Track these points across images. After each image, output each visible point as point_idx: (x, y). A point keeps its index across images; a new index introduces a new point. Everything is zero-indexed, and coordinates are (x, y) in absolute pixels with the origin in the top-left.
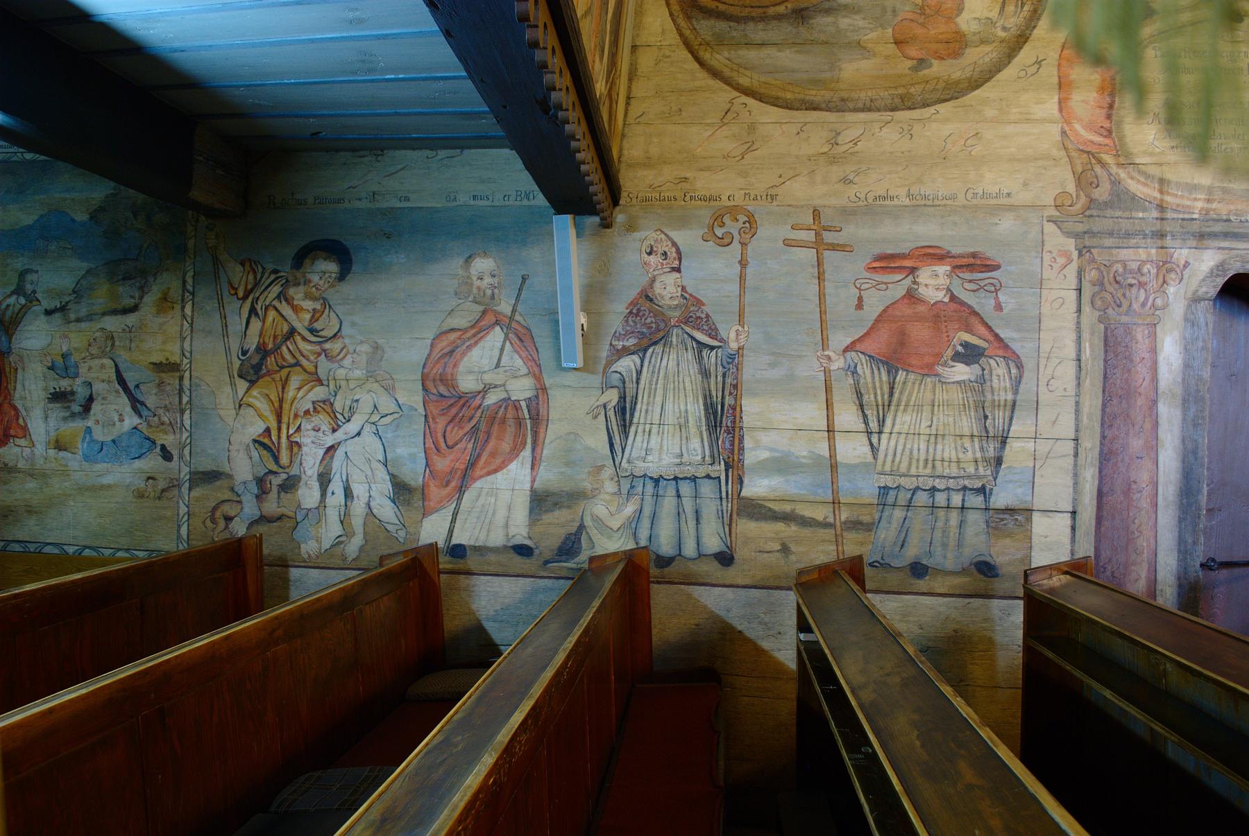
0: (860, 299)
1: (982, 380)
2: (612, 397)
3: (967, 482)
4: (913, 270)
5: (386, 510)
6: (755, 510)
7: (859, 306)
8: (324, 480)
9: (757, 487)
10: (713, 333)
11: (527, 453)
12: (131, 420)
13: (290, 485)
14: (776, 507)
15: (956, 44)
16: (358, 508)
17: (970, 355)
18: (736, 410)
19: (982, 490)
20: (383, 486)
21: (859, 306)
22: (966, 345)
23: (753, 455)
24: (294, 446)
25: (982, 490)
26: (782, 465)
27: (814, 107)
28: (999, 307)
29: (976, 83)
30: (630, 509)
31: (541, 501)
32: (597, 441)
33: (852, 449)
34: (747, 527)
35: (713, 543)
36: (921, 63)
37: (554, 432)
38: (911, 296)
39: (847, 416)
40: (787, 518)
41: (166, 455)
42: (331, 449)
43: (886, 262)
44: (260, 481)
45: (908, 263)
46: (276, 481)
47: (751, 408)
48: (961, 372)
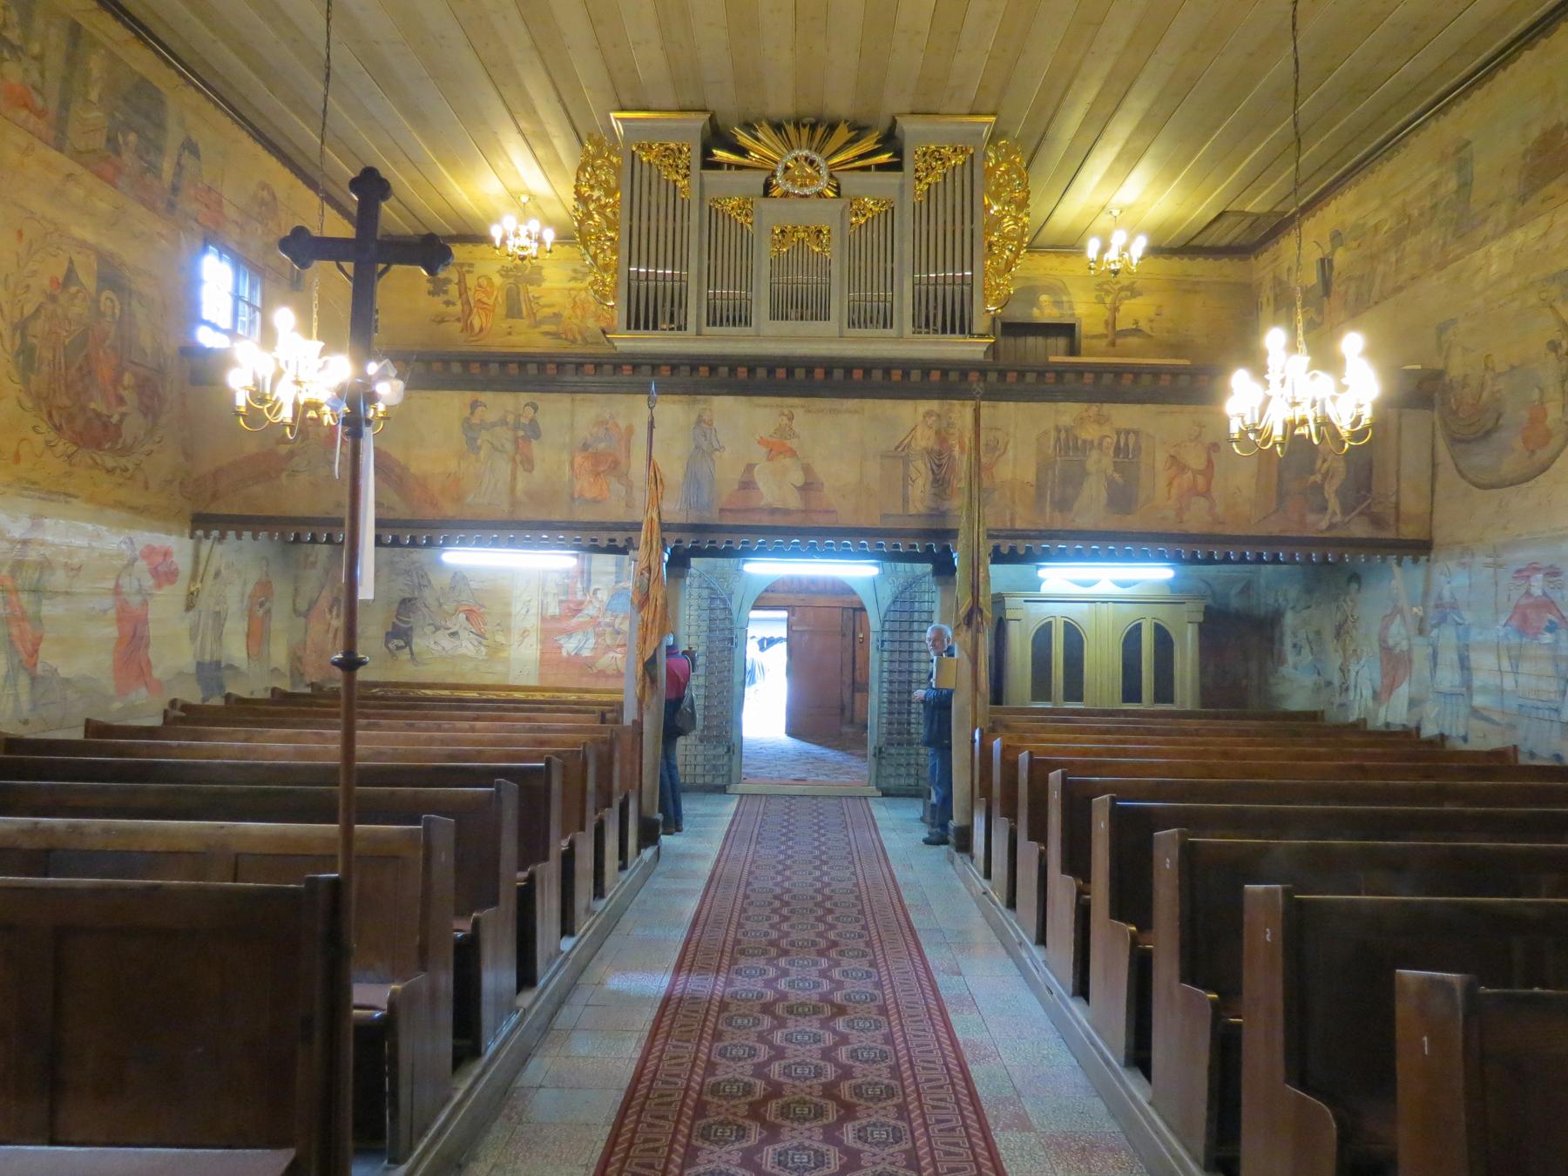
0: (1509, 596)
1: (1557, 642)
2: (1430, 650)
3: (1551, 705)
4: (1529, 577)
5: (1370, 703)
6: (1475, 712)
7: (1509, 599)
8: (1356, 686)
9: (1478, 701)
10: (1461, 618)
11: (1407, 678)
12: (1310, 658)
13: (1347, 689)
14: (1485, 713)
15: (1549, 435)
16: (1363, 703)
17: (1552, 628)
18: (1468, 657)
19: (1557, 710)
20: (1370, 692)
21: (1509, 599)
22: (1550, 621)
23: (1476, 683)
24: (1349, 670)
25: (1557, 710)
26: (1485, 690)
27: (1492, 486)
28: (1563, 598)
29: (1553, 460)
30: (1437, 709)
31: (1413, 703)
32: (1427, 672)
33: (1509, 683)
34: (1476, 724)
35: (1462, 733)
36: (1533, 452)
37: (1416, 666)
38: (1528, 594)
39: (1506, 665)
40: (1487, 719)
41: (1319, 674)
42: (1357, 673)
43: (1524, 574)
44: (1341, 687)
45: (1526, 573)
46: (1344, 686)
47: (1473, 656)
48: (1547, 638)
